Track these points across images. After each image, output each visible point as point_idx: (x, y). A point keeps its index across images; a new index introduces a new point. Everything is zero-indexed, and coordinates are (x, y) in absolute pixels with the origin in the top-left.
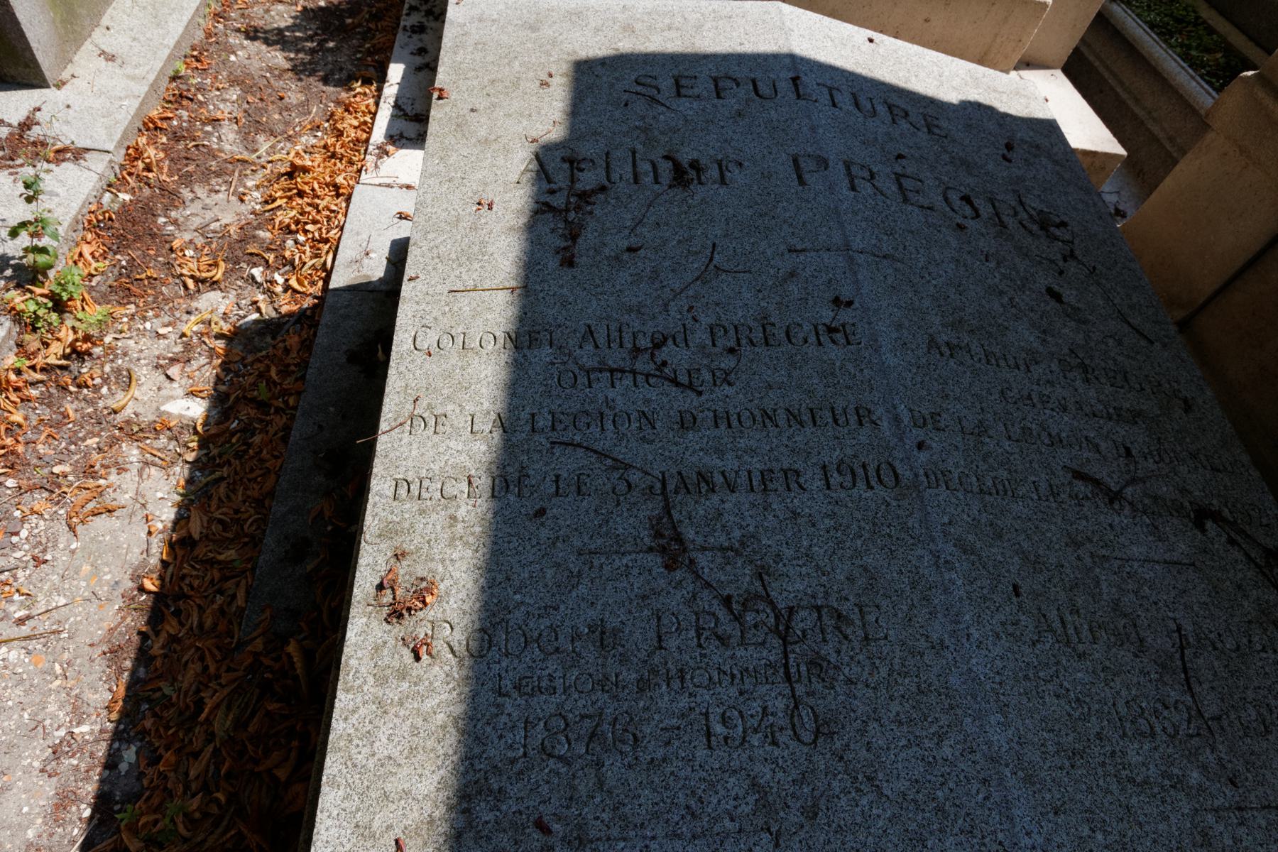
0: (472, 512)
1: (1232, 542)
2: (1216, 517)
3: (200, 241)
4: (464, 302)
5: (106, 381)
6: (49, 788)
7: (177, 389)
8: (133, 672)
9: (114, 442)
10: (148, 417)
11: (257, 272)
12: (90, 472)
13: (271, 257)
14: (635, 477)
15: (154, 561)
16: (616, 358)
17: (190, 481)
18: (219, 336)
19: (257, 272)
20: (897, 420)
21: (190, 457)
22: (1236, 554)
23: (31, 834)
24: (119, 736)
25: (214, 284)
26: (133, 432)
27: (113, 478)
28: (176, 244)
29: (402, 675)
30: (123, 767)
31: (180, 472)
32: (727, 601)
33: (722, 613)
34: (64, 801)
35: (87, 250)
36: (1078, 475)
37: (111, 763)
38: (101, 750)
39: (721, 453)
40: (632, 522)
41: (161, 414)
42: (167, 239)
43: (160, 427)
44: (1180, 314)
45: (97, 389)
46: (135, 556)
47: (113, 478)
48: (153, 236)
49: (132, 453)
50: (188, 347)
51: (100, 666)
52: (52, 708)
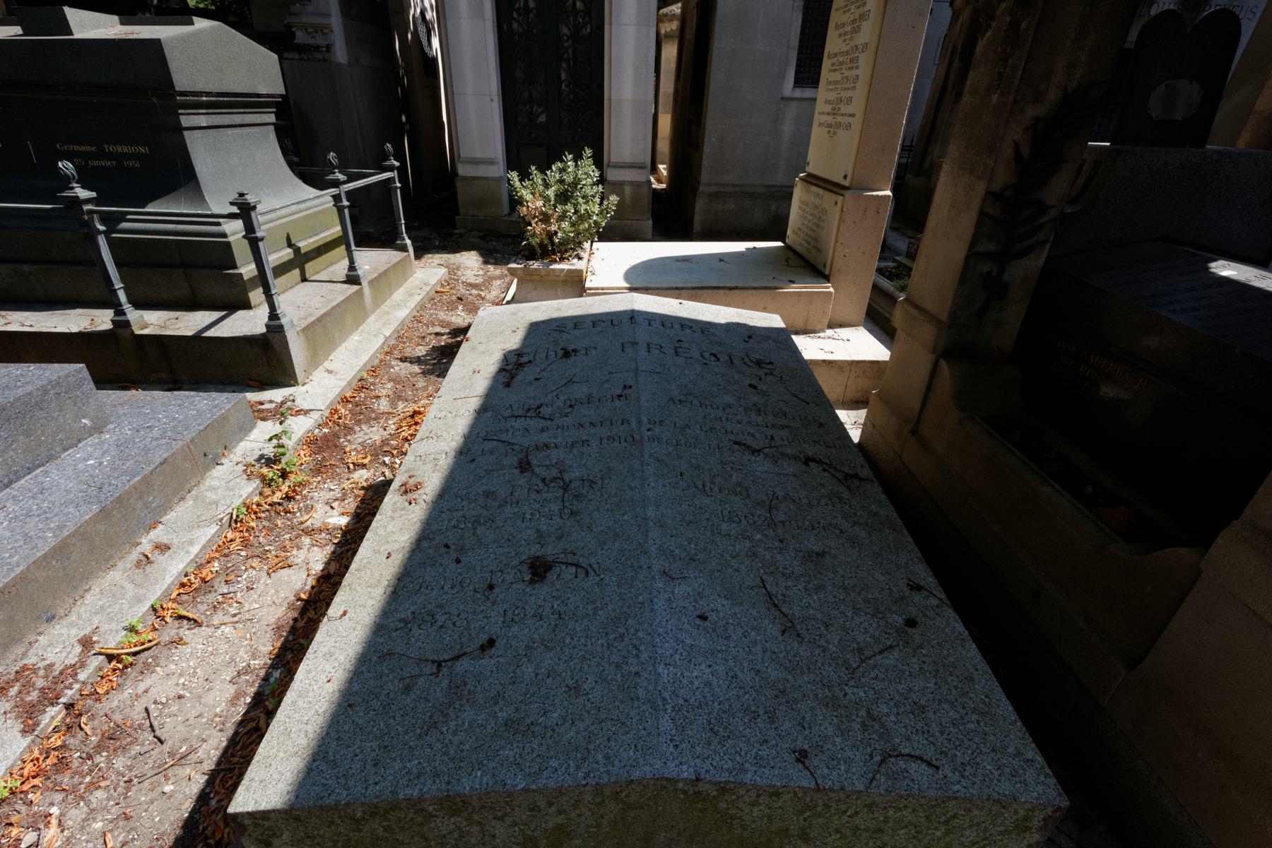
0: (445, 462)
1: (824, 470)
2: (814, 460)
3: (360, 448)
4: (459, 402)
5: (300, 510)
6: (232, 690)
7: (335, 512)
8: (286, 638)
9: (298, 536)
10: (318, 524)
11: (387, 459)
12: (284, 549)
13: (395, 452)
14: (516, 447)
15: (308, 588)
16: (520, 412)
17: (333, 553)
18: (363, 488)
19: (387, 459)
20: (640, 422)
21: (336, 541)
22: (826, 474)
23: (218, 710)
24: (273, 666)
25: (364, 466)
26: (309, 532)
27: (295, 552)
28: (347, 449)
29: (403, 509)
30: (272, 680)
31: (330, 549)
32: (544, 480)
33: (541, 484)
34: (237, 696)
35: (302, 453)
36: (736, 443)
37: (266, 679)
38: (262, 673)
39: (556, 438)
40: (512, 460)
41: (324, 523)
42: (343, 448)
43: (325, 529)
44: (910, 426)
45: (294, 513)
46: (298, 586)
47: (295, 552)
48: (336, 446)
49: (306, 540)
50: (345, 495)
51: (270, 634)
52: (241, 653)
